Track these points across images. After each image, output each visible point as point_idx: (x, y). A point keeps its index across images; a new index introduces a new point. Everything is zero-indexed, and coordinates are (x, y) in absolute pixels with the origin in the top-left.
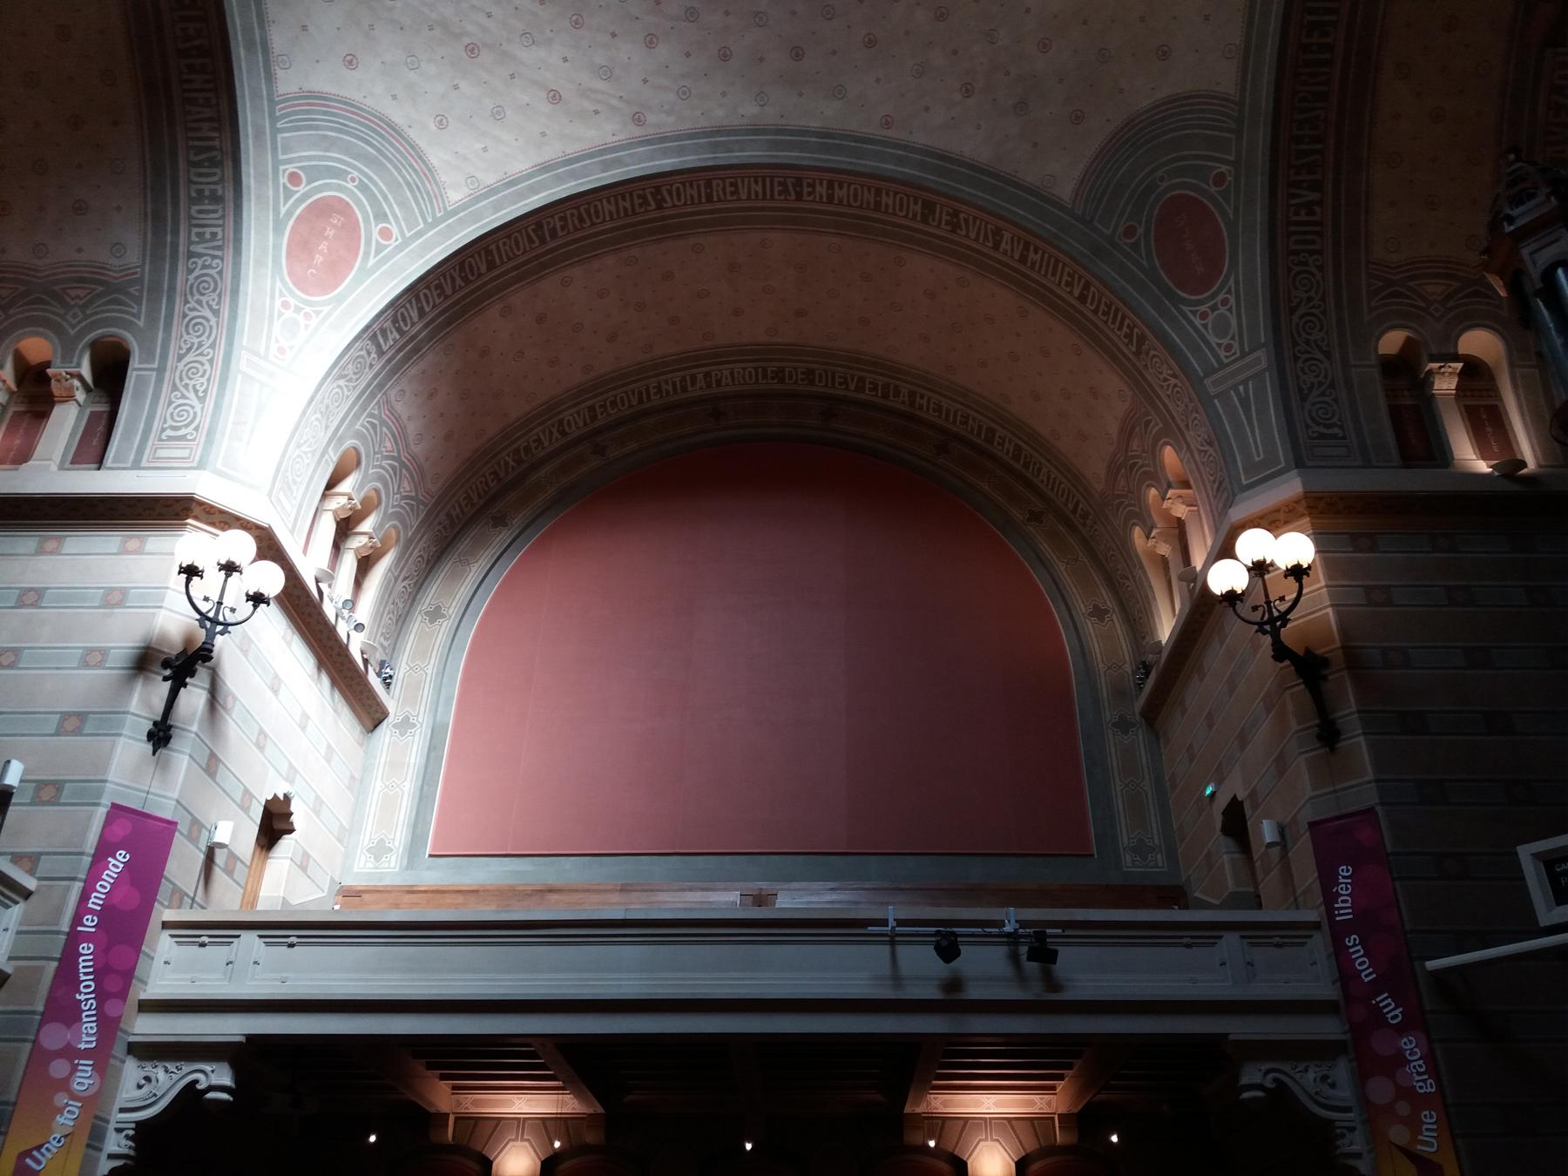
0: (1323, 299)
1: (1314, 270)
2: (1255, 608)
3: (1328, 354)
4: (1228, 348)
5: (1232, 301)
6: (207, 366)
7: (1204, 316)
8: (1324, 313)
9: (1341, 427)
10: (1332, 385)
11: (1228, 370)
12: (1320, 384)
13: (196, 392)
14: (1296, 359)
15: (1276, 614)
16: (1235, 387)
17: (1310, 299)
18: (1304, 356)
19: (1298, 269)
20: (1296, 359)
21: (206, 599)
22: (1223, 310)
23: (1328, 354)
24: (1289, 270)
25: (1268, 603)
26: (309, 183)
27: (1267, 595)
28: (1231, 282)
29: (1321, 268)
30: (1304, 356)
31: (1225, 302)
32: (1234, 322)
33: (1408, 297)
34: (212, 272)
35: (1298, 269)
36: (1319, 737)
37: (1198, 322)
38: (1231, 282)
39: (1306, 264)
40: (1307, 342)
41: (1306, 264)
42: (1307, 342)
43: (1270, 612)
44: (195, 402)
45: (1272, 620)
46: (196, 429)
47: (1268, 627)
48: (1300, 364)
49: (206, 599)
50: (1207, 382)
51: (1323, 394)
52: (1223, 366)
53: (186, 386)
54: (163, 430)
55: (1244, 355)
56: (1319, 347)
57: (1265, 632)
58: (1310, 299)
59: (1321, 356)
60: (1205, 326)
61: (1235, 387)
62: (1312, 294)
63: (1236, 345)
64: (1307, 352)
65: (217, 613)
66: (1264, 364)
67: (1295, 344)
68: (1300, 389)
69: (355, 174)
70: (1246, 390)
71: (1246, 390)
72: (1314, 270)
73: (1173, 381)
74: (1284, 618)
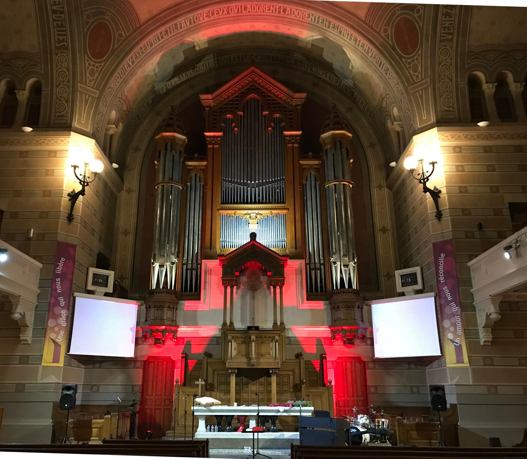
0: (451, 59)
1: (448, 48)
2: (419, 174)
4: (417, 76)
5: (420, 58)
6: (67, 89)
7: (410, 63)
8: (451, 64)
9: (453, 108)
10: (451, 92)
11: (416, 85)
12: (447, 91)
13: (64, 99)
14: (440, 82)
15: (425, 177)
16: (418, 91)
17: (446, 59)
20: (440, 82)
21: (81, 175)
22: (416, 62)
23: (451, 80)
25: (423, 173)
26: (93, 18)
27: (423, 170)
28: (420, 52)
29: (451, 47)
31: (417, 59)
32: (420, 67)
33: (480, 59)
34: (65, 55)
36: (436, 216)
37: (407, 65)
38: (420, 52)
39: (446, 46)
40: (444, 75)
41: (446, 46)
42: (444, 75)
43: (424, 176)
44: (65, 103)
45: (424, 179)
46: (66, 112)
47: (422, 181)
48: (440, 84)
49: (81, 175)
50: (409, 88)
51: (448, 95)
52: (415, 83)
53: (61, 97)
54: (56, 113)
55: (422, 80)
56: (448, 77)
57: (421, 183)
58: (446, 59)
59: (449, 81)
60: (410, 67)
61: (418, 91)
62: (447, 57)
63: (420, 76)
65: (84, 179)
66: (429, 84)
68: (440, 93)
69: (108, 13)
70: (422, 93)
71: (422, 93)
72: (449, 49)
73: (398, 86)
74: (427, 178)
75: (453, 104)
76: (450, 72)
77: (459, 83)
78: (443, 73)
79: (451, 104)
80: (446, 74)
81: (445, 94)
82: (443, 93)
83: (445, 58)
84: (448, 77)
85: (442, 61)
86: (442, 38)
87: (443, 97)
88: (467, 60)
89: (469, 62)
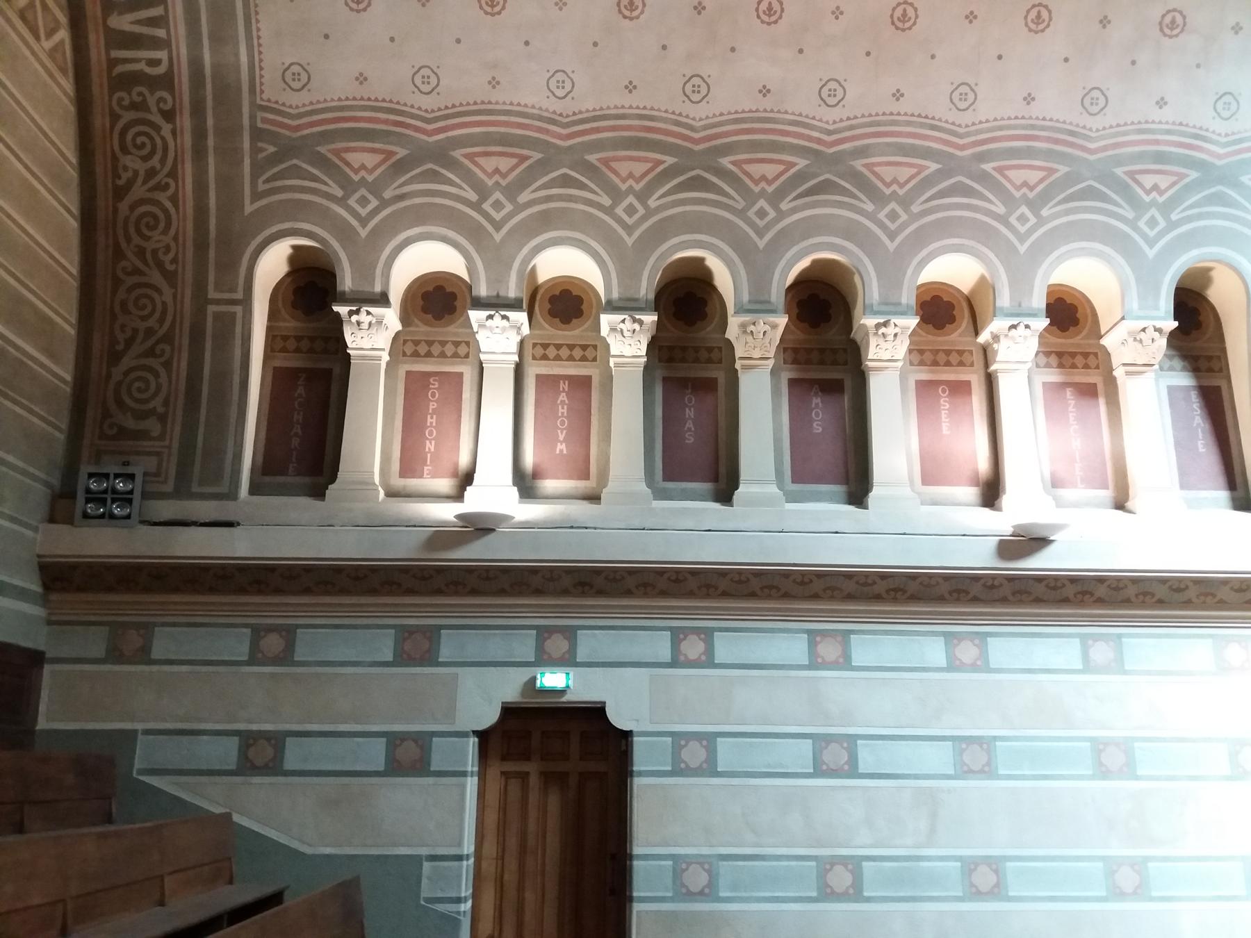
0: (173, 174)
3: (171, 278)
14: (117, 282)
17: (151, 173)
18: (131, 280)
19: (128, 116)
23: (171, 278)
24: (115, 117)
30: (131, 280)
35: (128, 116)
39: (140, 106)
40: (141, 253)
42: (141, 253)
62: (155, 161)
64: (137, 272)
67: (118, 254)
75: (166, 403)
76: (168, 239)
77: (212, 294)
78: (137, 240)
79: (157, 404)
80: (149, 246)
81: (137, 348)
82: (129, 342)
83: (142, 167)
84: (160, 265)
85: (130, 183)
86: (120, 69)
87: (127, 362)
88: (254, 178)
89: (261, 187)
